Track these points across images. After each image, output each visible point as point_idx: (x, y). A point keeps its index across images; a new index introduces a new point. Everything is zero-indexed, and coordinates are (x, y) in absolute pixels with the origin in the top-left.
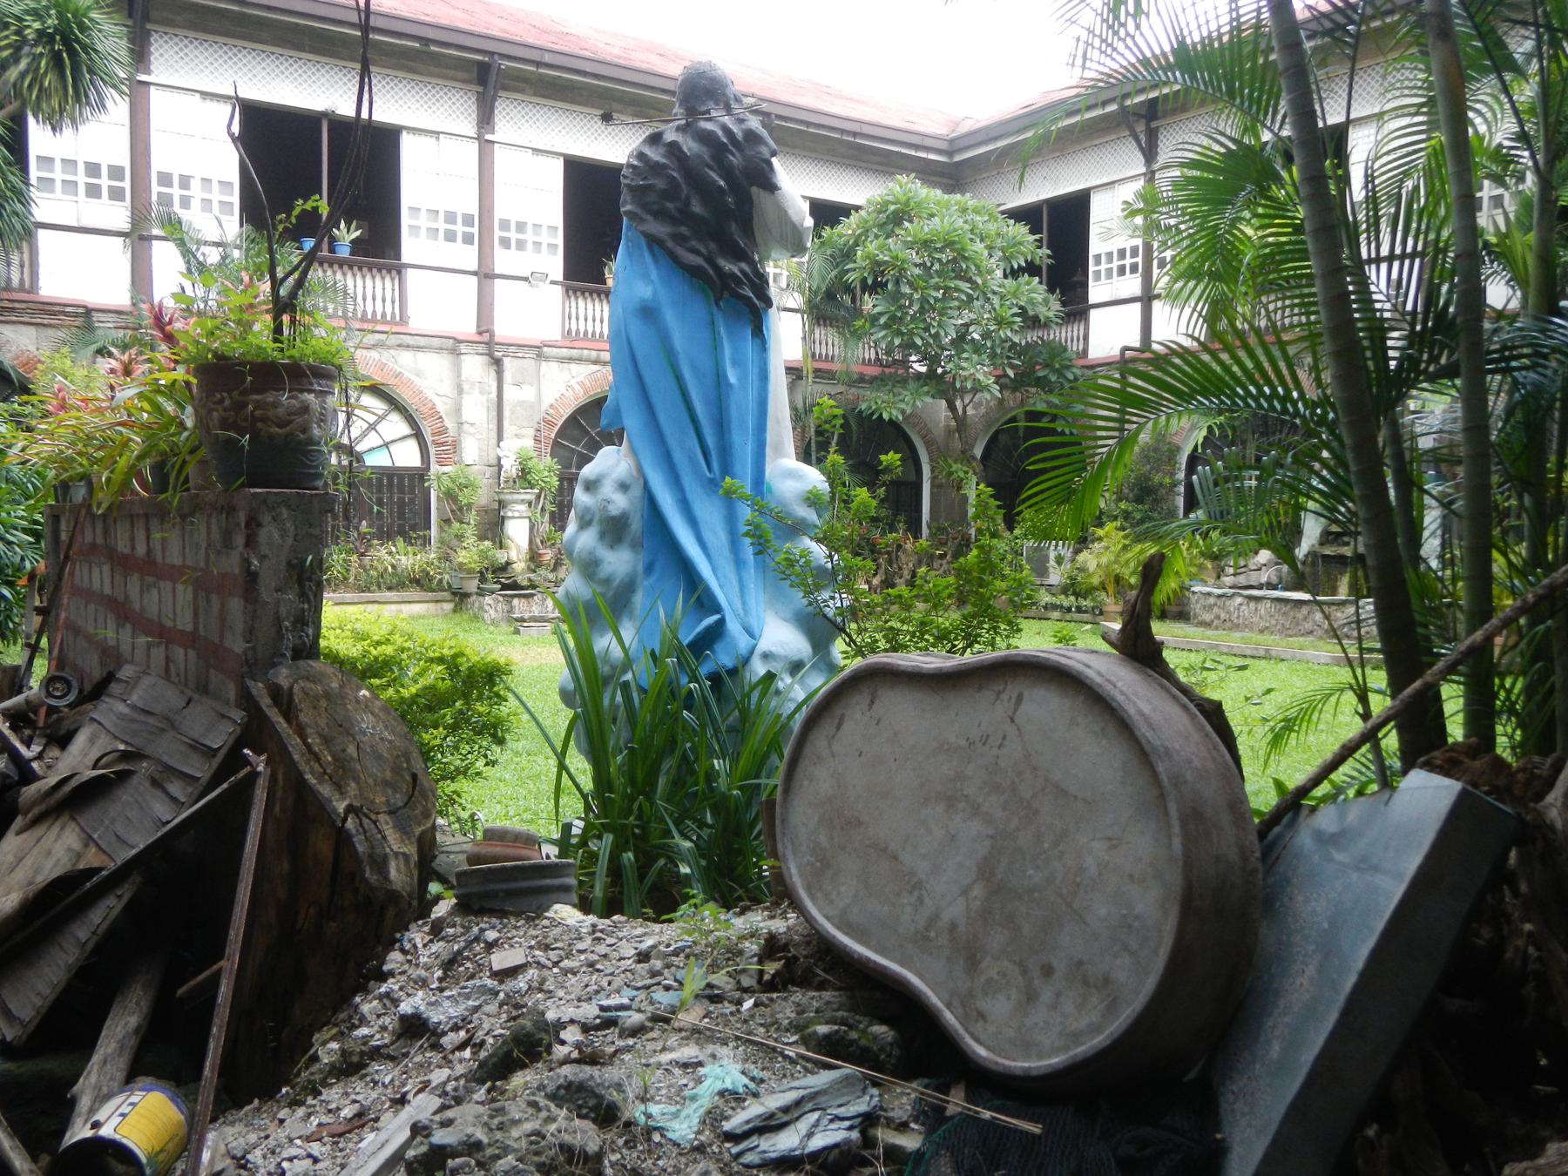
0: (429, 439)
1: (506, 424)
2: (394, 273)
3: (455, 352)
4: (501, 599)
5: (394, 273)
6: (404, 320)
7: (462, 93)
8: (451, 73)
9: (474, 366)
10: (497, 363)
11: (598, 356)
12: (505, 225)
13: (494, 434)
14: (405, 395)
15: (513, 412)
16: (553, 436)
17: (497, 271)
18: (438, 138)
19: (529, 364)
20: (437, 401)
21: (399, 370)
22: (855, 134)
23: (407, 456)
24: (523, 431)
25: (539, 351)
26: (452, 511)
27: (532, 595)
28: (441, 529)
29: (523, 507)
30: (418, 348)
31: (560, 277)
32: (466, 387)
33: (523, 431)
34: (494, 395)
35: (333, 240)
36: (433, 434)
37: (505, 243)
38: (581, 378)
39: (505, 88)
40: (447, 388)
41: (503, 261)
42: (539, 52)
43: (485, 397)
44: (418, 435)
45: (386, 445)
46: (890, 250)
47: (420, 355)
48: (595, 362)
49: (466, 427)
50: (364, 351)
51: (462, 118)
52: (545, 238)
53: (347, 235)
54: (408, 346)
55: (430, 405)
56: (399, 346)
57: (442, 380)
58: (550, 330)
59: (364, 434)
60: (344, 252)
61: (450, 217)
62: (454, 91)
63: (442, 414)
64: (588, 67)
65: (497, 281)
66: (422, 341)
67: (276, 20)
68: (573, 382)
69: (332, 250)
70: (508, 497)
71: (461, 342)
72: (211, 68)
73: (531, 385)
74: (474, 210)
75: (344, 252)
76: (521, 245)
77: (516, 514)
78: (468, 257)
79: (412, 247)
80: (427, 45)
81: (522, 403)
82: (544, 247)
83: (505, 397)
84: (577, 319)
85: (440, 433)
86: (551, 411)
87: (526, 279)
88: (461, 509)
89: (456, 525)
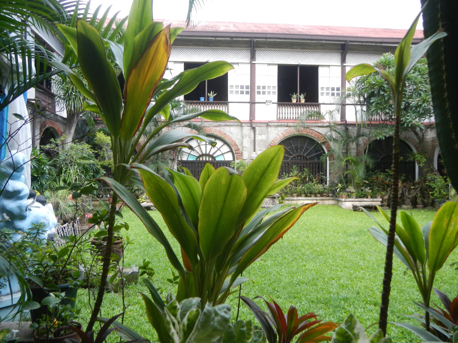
0: (234, 152)
1: (257, 147)
2: (225, 105)
3: (241, 126)
5: (225, 105)
7: (246, 51)
8: (242, 45)
9: (247, 130)
10: (254, 128)
11: (287, 124)
12: (259, 87)
14: (227, 140)
15: (259, 143)
17: (256, 101)
18: (238, 65)
19: (264, 128)
20: (236, 141)
21: (225, 132)
22: (381, 43)
25: (267, 124)
30: (231, 126)
31: (276, 101)
32: (244, 136)
34: (253, 138)
35: (208, 97)
36: (235, 151)
37: (259, 93)
38: (281, 132)
39: (259, 47)
40: (239, 137)
41: (258, 98)
42: (266, 35)
43: (250, 139)
44: (231, 151)
45: (223, 154)
46: (376, 80)
47: (232, 128)
48: (287, 126)
49: (244, 148)
50: (215, 128)
51: (246, 58)
52: (272, 90)
53: (212, 95)
54: (228, 125)
55: (234, 142)
56: (225, 125)
57: (238, 135)
58: (274, 118)
59: (216, 152)
60: (211, 100)
61: (242, 87)
62: (243, 50)
64: (282, 36)
65: (256, 104)
67: (193, 39)
68: (279, 133)
69: (208, 100)
71: (243, 123)
72: (177, 55)
73: (265, 134)
74: (249, 84)
75: (211, 100)
76: (264, 93)
78: (247, 98)
79: (231, 97)
80: (232, 38)
81: (262, 140)
82: (271, 93)
84: (282, 113)
85: (237, 150)
86: (272, 142)
87: (265, 103)
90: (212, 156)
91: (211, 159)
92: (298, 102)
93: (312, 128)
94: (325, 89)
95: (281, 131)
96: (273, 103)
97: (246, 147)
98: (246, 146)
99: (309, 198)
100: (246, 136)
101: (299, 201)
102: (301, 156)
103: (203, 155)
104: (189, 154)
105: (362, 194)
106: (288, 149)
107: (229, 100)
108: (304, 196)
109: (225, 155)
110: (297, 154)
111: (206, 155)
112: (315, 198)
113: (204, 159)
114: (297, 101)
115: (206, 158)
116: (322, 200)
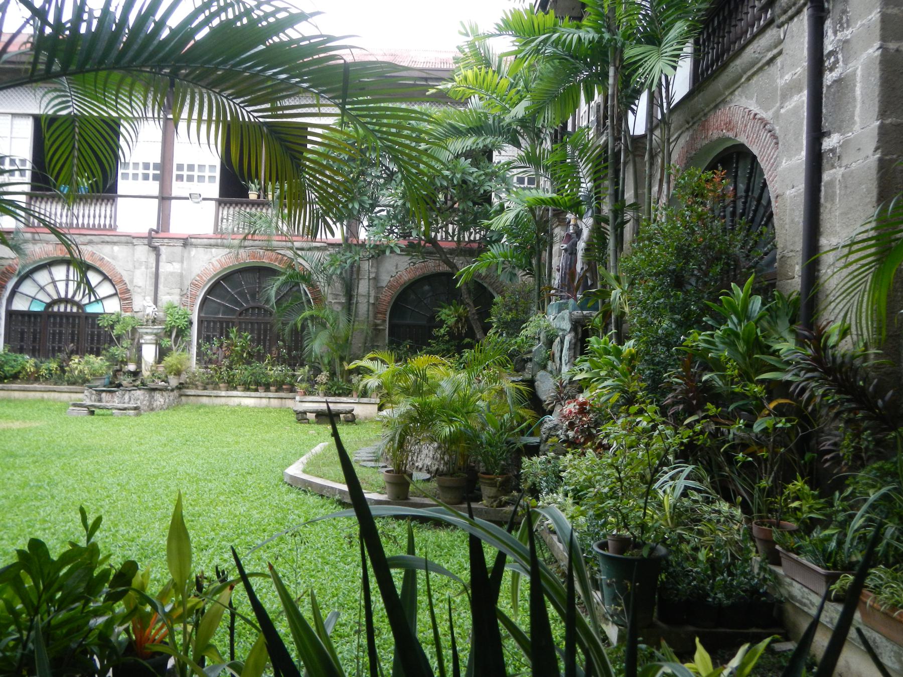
1: (161, 286)
6: (116, 227)
9: (142, 252)
10: (156, 249)
12: (180, 167)
17: (173, 195)
19: (179, 250)
21: (102, 256)
23: (112, 306)
24: (173, 291)
27: (115, 392)
30: (115, 243)
33: (173, 291)
34: (154, 269)
37: (180, 178)
38: (219, 257)
41: (178, 188)
47: (116, 248)
52: (207, 173)
53: (85, 184)
54: (108, 242)
61: (146, 166)
63: (127, 281)
65: (173, 201)
66: (115, 239)
68: (214, 261)
71: (134, 238)
76: (190, 179)
79: (123, 186)
81: (172, 274)
83: (161, 270)
90: (78, 304)
91: (75, 310)
92: (262, 199)
93: (282, 252)
94: (141, 166)
95: (217, 255)
96: (204, 199)
99: (253, 394)
100: (141, 263)
101: (219, 399)
102: (259, 308)
103: (59, 301)
104: (34, 298)
105: (337, 389)
106: (236, 293)
107: (120, 192)
109: (106, 302)
110: (252, 304)
111: (66, 301)
112: (263, 394)
113: (62, 309)
114: (259, 197)
115: (66, 308)
116: (281, 398)
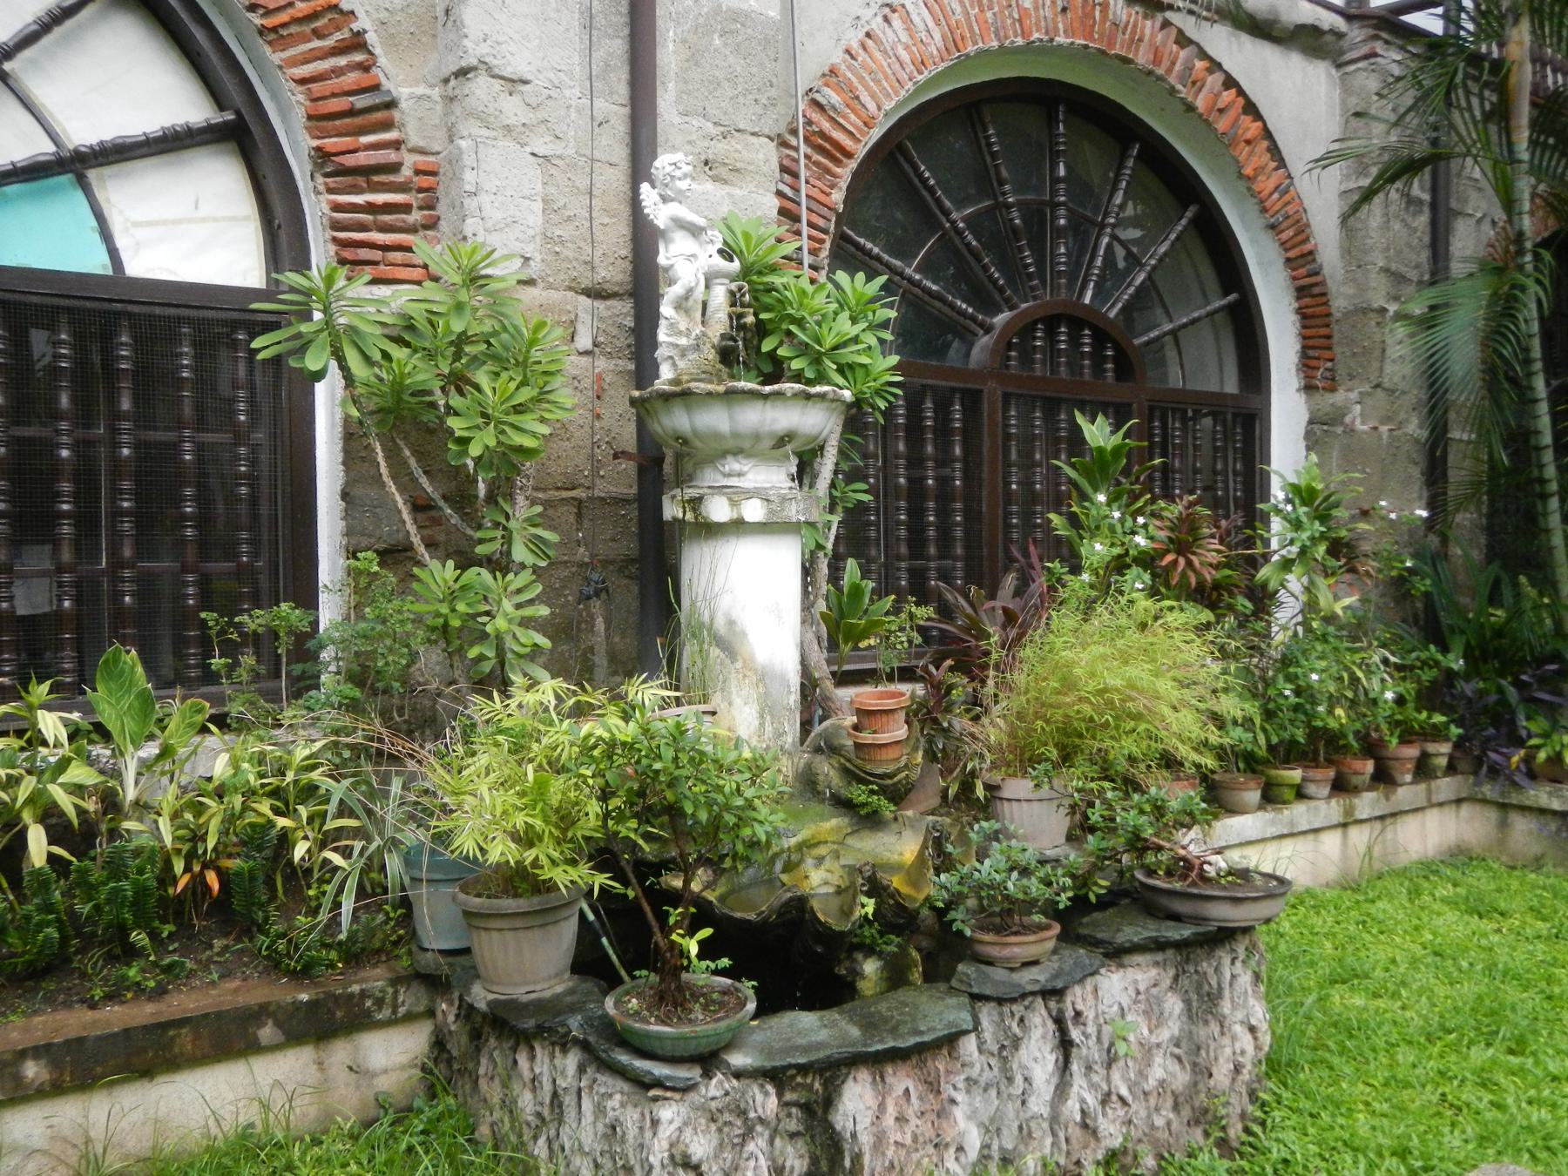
4: (766, 1102)
13: (614, 147)
15: (694, 58)
16: (838, 197)
26: (420, 507)
28: (360, 587)
29: (774, 477)
49: (481, 88)
63: (362, 23)
70: (715, 419)
77: (754, 511)
86: (832, 97)
88: (462, 499)
89: (440, 573)
97: (515, 83)
98: (517, 65)
102: (1077, 321)
108: (1254, 796)
